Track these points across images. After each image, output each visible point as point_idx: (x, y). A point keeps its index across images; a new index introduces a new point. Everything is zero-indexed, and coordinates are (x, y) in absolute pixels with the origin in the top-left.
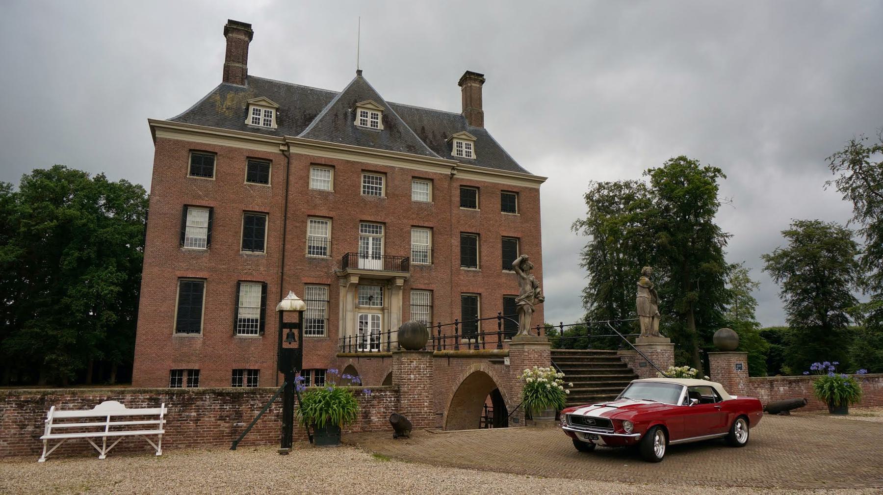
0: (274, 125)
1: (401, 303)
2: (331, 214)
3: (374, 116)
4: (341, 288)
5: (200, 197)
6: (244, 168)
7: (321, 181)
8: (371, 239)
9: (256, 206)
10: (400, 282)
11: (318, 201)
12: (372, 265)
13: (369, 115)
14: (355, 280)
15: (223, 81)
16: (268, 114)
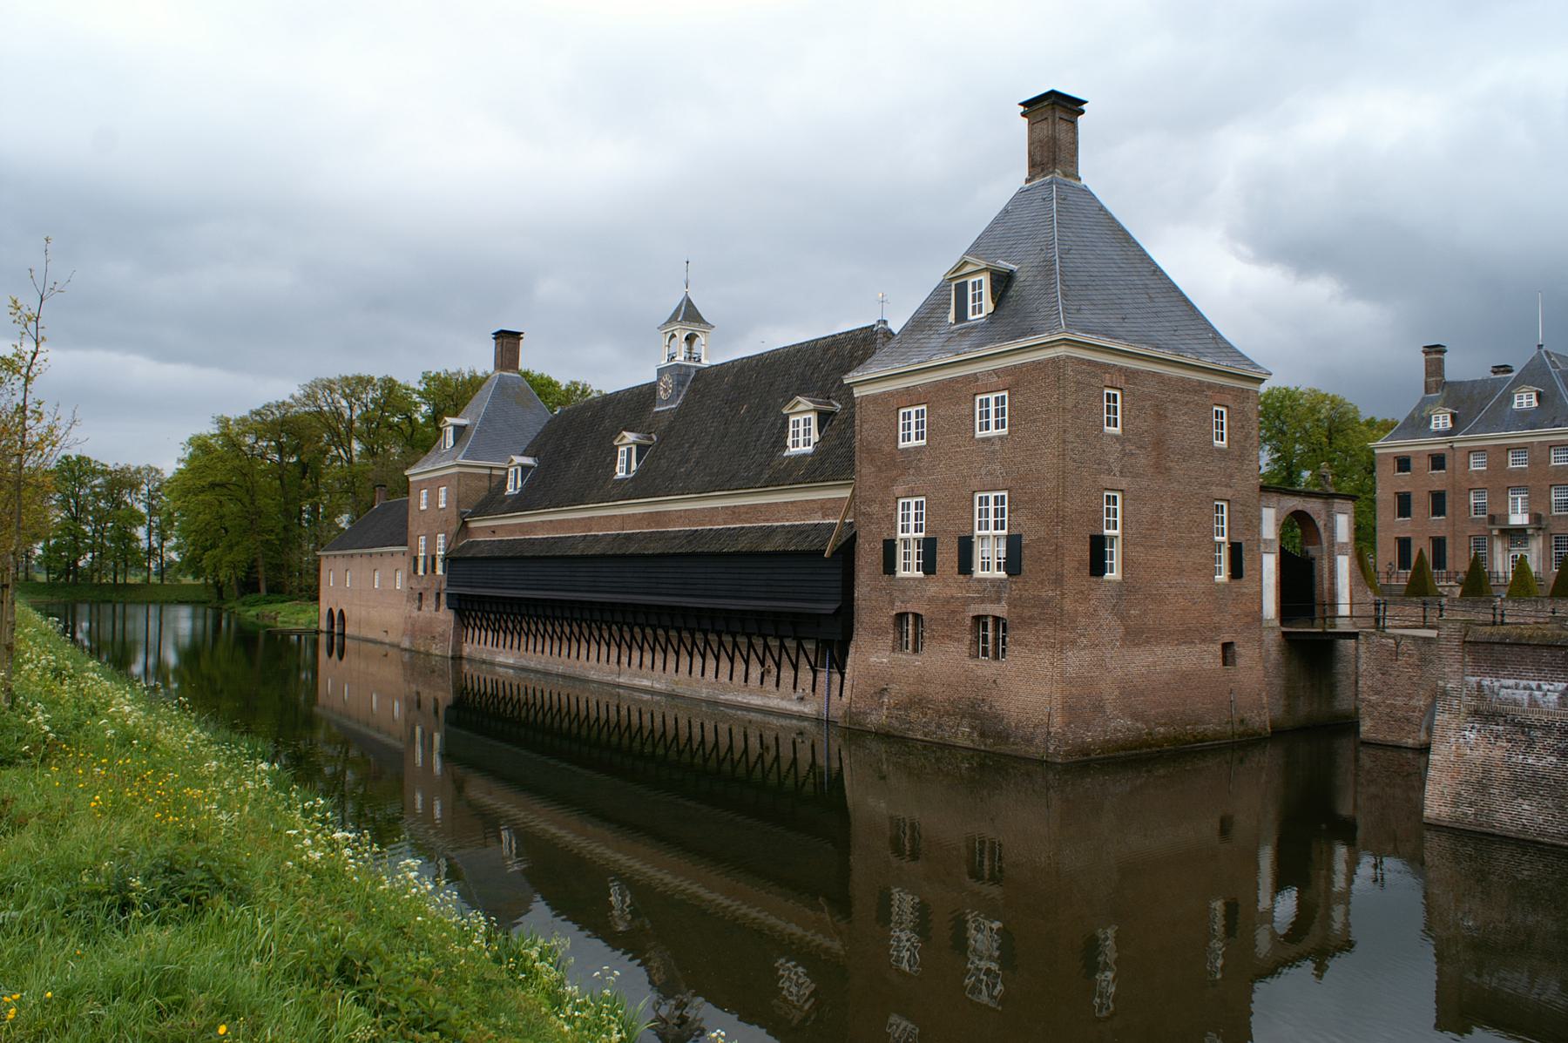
0: (1450, 425)
1: (1541, 546)
2: (1486, 486)
3: (1529, 397)
4: (1495, 538)
5: (1402, 487)
6: (1427, 462)
7: (1476, 465)
8: (1519, 500)
9: (1437, 488)
10: (1530, 532)
11: (1475, 478)
12: (1518, 519)
13: (1525, 397)
14: (1495, 532)
15: (1427, 392)
16: (1444, 418)
